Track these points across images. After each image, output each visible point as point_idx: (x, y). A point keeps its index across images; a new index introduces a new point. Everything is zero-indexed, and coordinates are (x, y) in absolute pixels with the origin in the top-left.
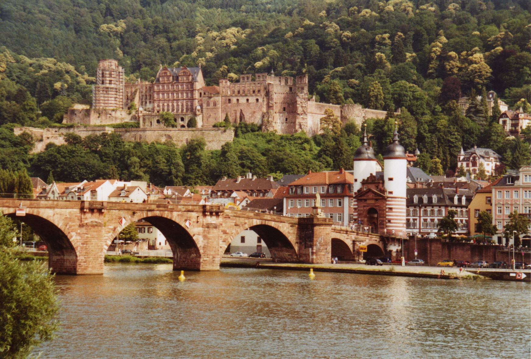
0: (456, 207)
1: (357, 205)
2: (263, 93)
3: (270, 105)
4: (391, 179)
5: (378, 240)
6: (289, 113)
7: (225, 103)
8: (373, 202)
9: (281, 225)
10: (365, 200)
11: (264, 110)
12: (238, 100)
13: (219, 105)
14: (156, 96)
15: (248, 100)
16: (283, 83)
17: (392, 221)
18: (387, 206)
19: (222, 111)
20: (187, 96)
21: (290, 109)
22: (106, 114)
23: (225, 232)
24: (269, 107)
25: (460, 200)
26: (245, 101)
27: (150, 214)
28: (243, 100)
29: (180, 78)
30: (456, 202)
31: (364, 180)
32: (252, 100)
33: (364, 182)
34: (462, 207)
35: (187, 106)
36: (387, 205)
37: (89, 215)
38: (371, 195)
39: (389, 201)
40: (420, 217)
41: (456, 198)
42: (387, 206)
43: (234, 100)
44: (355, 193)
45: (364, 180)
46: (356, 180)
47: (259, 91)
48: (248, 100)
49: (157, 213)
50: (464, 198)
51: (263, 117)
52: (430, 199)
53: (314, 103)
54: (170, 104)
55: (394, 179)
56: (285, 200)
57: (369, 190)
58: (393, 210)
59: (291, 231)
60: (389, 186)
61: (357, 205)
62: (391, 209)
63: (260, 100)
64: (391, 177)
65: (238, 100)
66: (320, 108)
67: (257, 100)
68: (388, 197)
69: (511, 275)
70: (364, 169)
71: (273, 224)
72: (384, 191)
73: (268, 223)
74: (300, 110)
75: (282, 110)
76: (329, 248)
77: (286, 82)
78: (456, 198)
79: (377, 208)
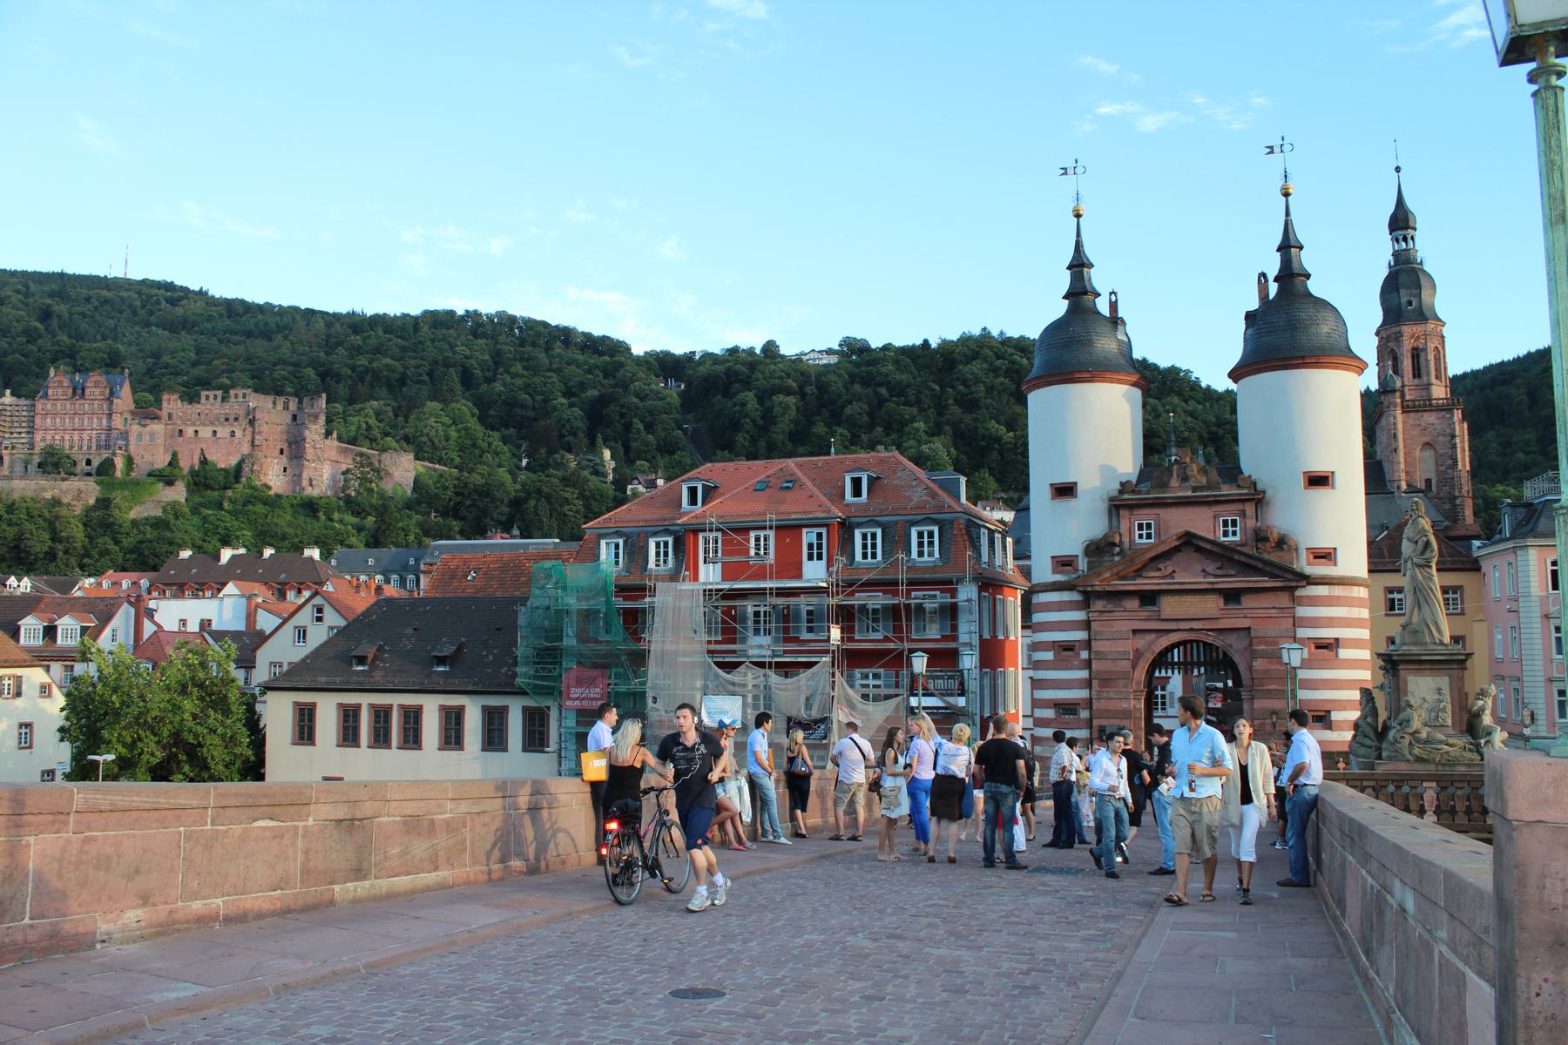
1: (1087, 625)
2: (244, 422)
4: (1319, 481)
10: (1149, 598)
11: (246, 449)
15: (215, 432)
16: (280, 406)
17: (1335, 716)
18: (1302, 633)
21: (295, 449)
28: (205, 432)
29: (87, 391)
32: (223, 432)
33: (1121, 503)
36: (1297, 622)
39: (1315, 601)
42: (1302, 633)
43: (190, 431)
44: (1063, 563)
47: (236, 419)
48: (215, 432)
53: (336, 443)
54: (67, 437)
55: (1339, 480)
58: (1344, 653)
61: (1087, 625)
62: (1322, 645)
63: (239, 434)
64: (1320, 467)
66: (344, 451)
67: (233, 434)
68: (1310, 580)
74: (310, 453)
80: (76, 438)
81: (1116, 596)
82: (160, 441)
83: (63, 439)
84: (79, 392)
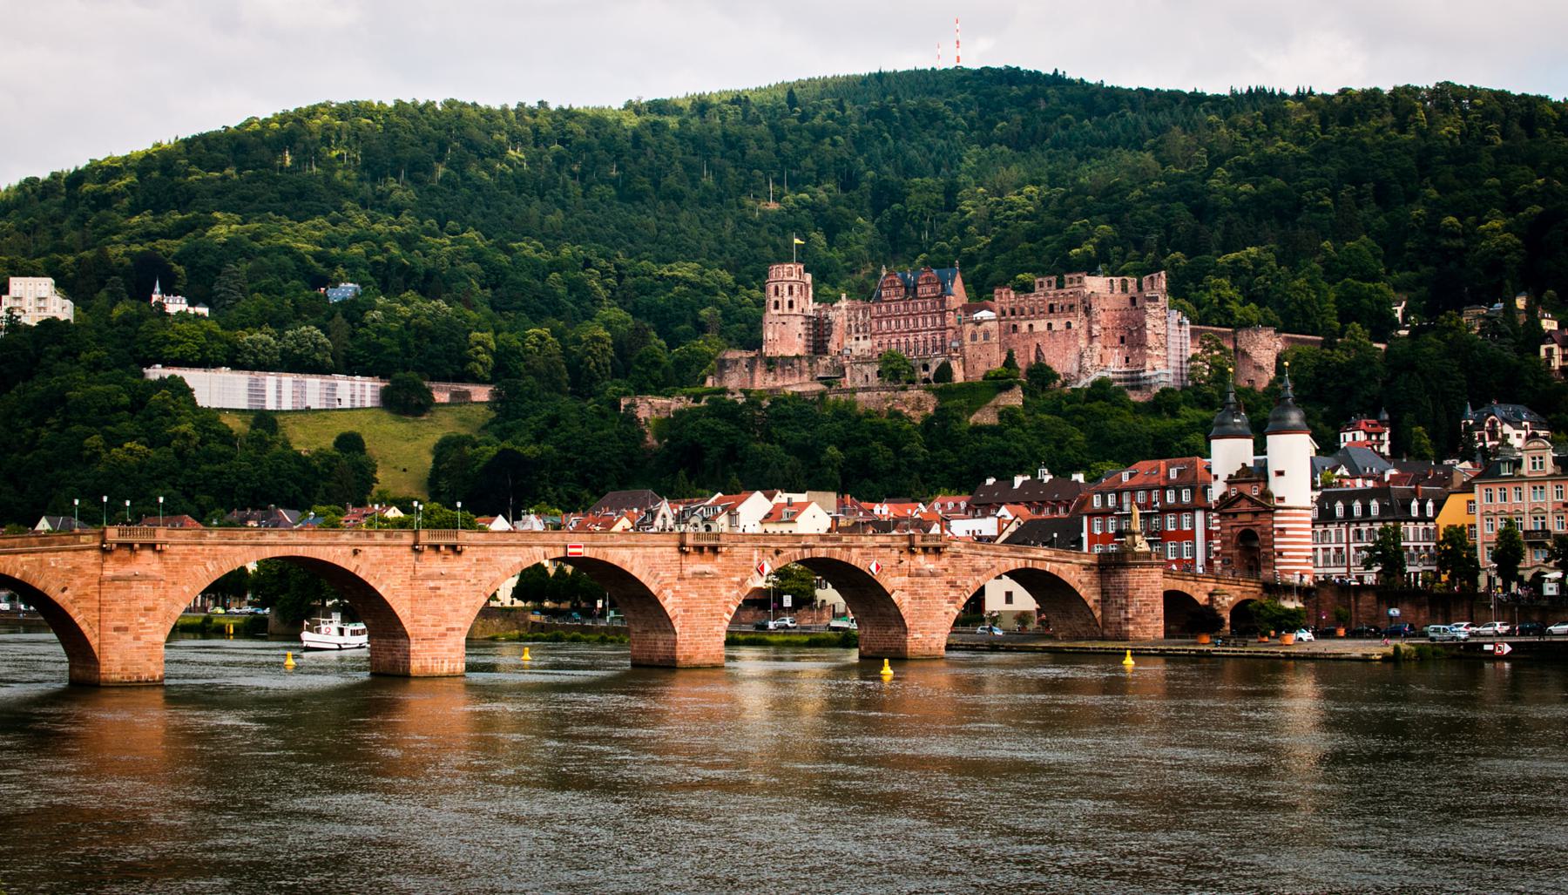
0: (1416, 520)
3: (1095, 333)
4: (1280, 473)
5: (1260, 591)
6: (1132, 347)
7: (1007, 333)
8: (1248, 518)
9: (1063, 567)
10: (1235, 515)
12: (1031, 326)
13: (994, 339)
14: (874, 325)
15: (1050, 326)
19: (1002, 349)
20: (934, 323)
21: (1132, 337)
22: (782, 366)
23: (953, 585)
24: (1091, 338)
25: (1422, 508)
26: (1045, 328)
27: (807, 554)
28: (1040, 325)
29: (919, 290)
30: (1415, 513)
31: (1230, 476)
32: (1058, 324)
33: (1231, 481)
34: (1427, 520)
35: (934, 341)
37: (695, 557)
38: (1244, 506)
40: (1348, 543)
41: (1415, 504)
43: (1024, 326)
45: (1230, 476)
46: (1216, 477)
47: (1071, 307)
48: (1050, 326)
49: (822, 553)
50: (1430, 505)
51: (1081, 356)
52: (1366, 509)
54: (903, 340)
56: (1085, 519)
57: (1241, 496)
59: (1085, 580)
60: (1276, 486)
62: (1282, 530)
65: (1031, 326)
67: (1069, 325)
69: (1487, 647)
70: (1228, 455)
71: (1048, 567)
72: (1266, 495)
73: (1038, 565)
74: (1151, 340)
75: (1117, 341)
76: (1160, 609)
77: (1124, 289)
78: (1415, 504)
79: (1257, 530)
80: (911, 340)
81: (1227, 514)
82: (994, 339)
83: (898, 343)
84: (911, 290)
